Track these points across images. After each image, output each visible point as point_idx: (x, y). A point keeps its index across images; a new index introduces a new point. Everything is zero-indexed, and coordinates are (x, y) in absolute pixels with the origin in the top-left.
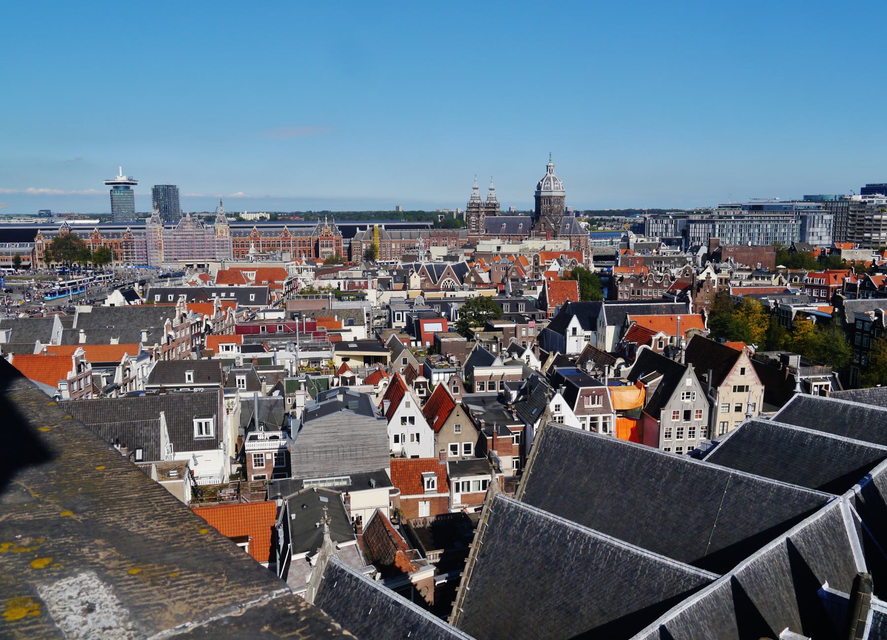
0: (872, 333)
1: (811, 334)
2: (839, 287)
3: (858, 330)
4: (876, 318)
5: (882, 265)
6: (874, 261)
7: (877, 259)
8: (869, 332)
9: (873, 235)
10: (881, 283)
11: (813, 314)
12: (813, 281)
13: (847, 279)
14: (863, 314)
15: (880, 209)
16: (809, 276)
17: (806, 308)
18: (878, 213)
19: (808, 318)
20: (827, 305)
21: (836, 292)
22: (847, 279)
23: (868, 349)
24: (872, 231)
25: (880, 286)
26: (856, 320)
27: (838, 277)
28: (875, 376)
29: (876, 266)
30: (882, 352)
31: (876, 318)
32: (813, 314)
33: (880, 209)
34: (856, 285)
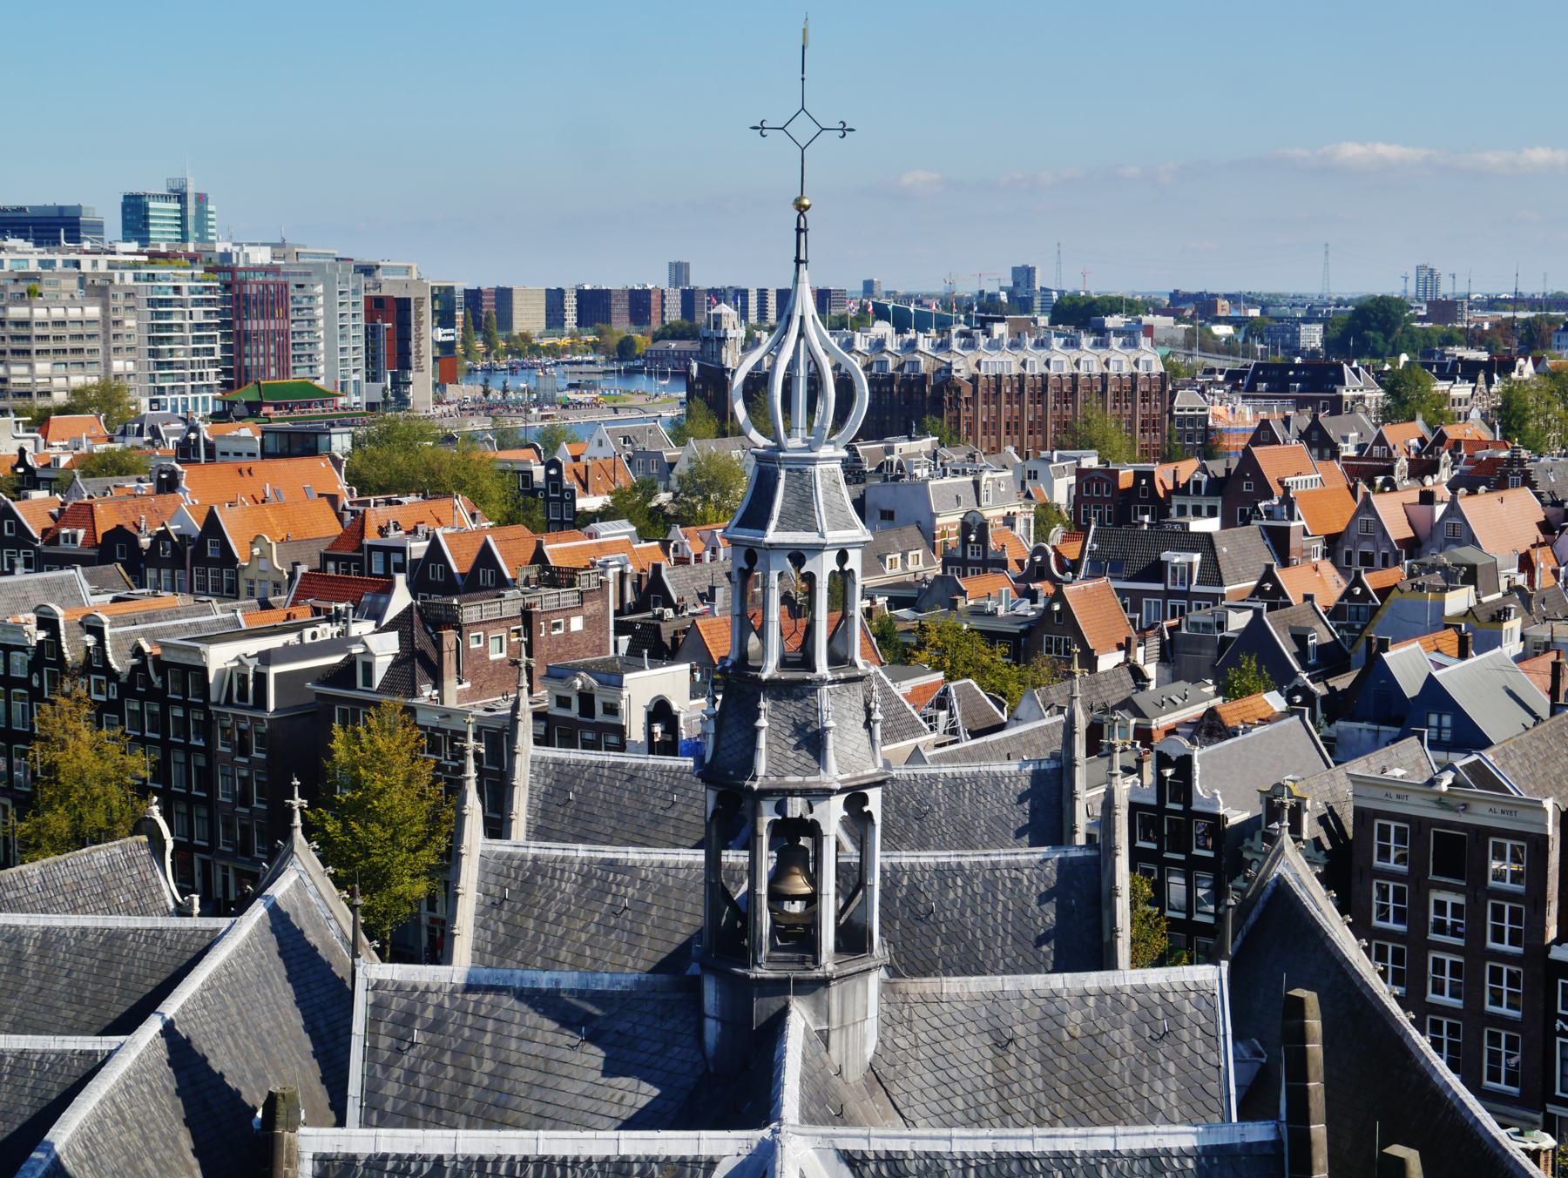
0: (35, 683)
4: (42, 635)
5: (48, 466)
6: (22, 452)
7: (29, 447)
8: (25, 683)
9: (14, 370)
10: (49, 523)
15: (23, 287)
18: (21, 299)
23: (29, 737)
24: (9, 357)
25: (45, 532)
28: (58, 821)
29: (30, 470)
30: (71, 741)
31: (42, 635)
33: (23, 287)
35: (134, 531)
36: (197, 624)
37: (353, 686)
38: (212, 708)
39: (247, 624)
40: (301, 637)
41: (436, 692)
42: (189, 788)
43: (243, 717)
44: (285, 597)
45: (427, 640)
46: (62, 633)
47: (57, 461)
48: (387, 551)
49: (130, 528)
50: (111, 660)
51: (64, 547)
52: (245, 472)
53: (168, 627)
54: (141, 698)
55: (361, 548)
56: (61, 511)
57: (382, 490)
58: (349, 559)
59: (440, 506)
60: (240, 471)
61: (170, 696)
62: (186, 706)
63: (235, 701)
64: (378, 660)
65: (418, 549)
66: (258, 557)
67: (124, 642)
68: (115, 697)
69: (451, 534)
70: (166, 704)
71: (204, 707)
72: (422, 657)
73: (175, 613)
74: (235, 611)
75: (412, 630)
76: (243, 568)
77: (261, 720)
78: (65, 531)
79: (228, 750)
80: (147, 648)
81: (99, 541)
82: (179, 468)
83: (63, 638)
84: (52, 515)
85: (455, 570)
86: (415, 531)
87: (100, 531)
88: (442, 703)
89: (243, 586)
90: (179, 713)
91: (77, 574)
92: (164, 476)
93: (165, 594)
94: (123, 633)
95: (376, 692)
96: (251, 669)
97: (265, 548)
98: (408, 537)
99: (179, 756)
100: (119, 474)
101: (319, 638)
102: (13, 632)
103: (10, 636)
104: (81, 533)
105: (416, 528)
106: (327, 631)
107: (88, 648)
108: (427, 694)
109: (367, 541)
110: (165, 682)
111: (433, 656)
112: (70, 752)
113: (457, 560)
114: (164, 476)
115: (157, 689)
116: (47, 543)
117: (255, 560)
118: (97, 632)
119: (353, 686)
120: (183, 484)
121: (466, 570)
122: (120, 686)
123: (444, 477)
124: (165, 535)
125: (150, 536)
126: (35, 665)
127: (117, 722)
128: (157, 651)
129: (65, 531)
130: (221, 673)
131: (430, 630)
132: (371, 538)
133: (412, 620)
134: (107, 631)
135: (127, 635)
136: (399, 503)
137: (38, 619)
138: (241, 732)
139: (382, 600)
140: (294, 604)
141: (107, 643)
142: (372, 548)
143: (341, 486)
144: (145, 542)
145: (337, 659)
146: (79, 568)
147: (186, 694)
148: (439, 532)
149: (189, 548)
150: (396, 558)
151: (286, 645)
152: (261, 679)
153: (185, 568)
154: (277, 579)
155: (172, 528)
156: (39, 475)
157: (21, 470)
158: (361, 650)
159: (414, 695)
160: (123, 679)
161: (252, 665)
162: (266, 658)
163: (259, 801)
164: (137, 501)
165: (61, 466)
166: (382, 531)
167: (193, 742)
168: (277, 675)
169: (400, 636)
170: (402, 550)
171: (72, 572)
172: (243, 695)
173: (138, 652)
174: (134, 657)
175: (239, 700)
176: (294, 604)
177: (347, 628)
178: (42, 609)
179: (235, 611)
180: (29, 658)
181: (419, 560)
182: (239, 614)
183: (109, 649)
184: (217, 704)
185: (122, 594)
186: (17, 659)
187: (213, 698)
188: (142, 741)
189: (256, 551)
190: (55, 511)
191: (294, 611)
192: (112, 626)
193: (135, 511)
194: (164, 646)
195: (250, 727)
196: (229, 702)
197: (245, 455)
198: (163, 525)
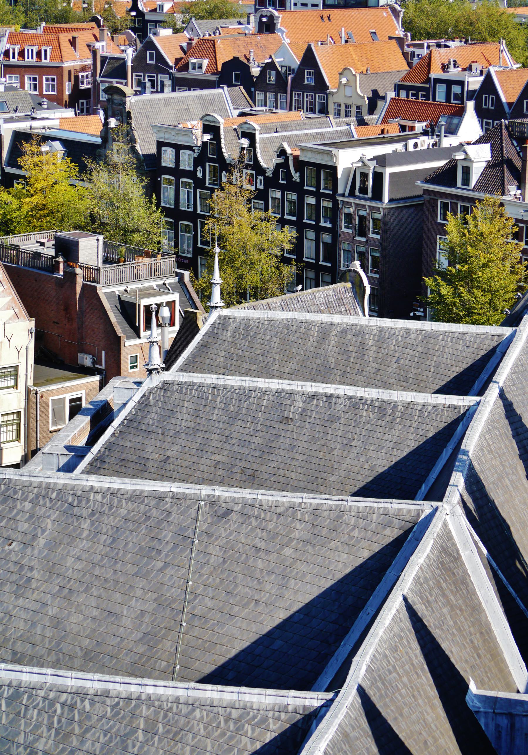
0: (200, 175)
1: (63, 187)
2: (84, 69)
3: (167, 171)
4: (207, 137)
5: (154, 10)
8: (192, 174)
10: (181, 55)
11: (54, 139)
12: (22, 54)
13: (98, 45)
14: (174, 128)
16: (11, 41)
17: (35, 124)
19: (45, 148)
20: (69, 113)
21: (77, 78)
22: (98, 45)
25: (178, 61)
26: (160, 145)
27: (78, 42)
30: (236, 219)
31: (207, 137)
32: (54, 139)
34: (123, 62)
35: (245, 61)
36: (322, 134)
37: (453, 184)
38: (338, 198)
39: (358, 135)
40: (406, 146)
41: (519, 192)
42: (317, 259)
43: (364, 206)
44: (377, 116)
45: (514, 152)
46: (222, 136)
47: (161, 7)
48: (449, 83)
49: (243, 59)
50: (260, 159)
51: (192, 74)
52: (326, 18)
53: (301, 135)
54: (283, 189)
55: (428, 80)
56: (189, 45)
57: (430, 36)
58: (418, 89)
59: (489, 49)
60: (322, 18)
61: (305, 188)
62: (318, 195)
63: (357, 193)
64: (475, 165)
65: (475, 82)
66: (345, 85)
67: (269, 145)
68: (262, 187)
69: (501, 72)
70: (302, 194)
71: (333, 197)
72: (509, 163)
73: (301, 126)
74: (349, 125)
75: (502, 142)
76: (333, 94)
77: (378, 209)
78: (193, 60)
79: (350, 231)
80: (289, 151)
81: (220, 69)
82: (276, 13)
83: (222, 141)
84: (182, 48)
85: (504, 100)
86: (470, 68)
87: (220, 62)
88: (524, 200)
89: (332, 107)
90: (312, 200)
91: (224, 92)
92: (264, 20)
93: (282, 111)
94: (268, 138)
95: (473, 191)
96: (372, 169)
97: (351, 78)
98: (466, 73)
99: (310, 234)
100: (221, 17)
101: (419, 148)
102: (183, 135)
103: (181, 138)
104: (205, 63)
105: (471, 66)
106: (425, 142)
107: (242, 149)
108: (512, 193)
109: (433, 75)
110: (302, 177)
111: (518, 164)
112: (236, 226)
113: (505, 92)
114: (264, 20)
115: (296, 182)
116: (180, 70)
117: (342, 87)
118: (251, 137)
119: (453, 184)
120: (279, 26)
121: (514, 99)
122: (266, 179)
123: (481, 27)
124: (271, 66)
125: (258, 66)
126: (199, 162)
127: (262, 207)
128: (297, 153)
129: (193, 60)
130: (347, 171)
131: (516, 144)
132: (436, 73)
133: (502, 135)
134: (258, 137)
135: (271, 140)
136: (446, 46)
137: (204, 125)
138: (362, 218)
139: (455, 121)
140: (385, 121)
141: (258, 145)
142: (437, 81)
143: (400, 32)
144: (255, 71)
145: (440, 164)
146: (226, 87)
147: (318, 187)
148: (493, 70)
149: (290, 78)
150: (456, 89)
151: (395, 152)
152: (378, 177)
153: (286, 92)
154: (359, 103)
155: (277, 60)
156: (147, 18)
157: (133, 13)
158: (462, 157)
159: (503, 193)
160: (269, 174)
161: (372, 165)
162: (381, 160)
163: (371, 272)
164: (247, 39)
165: (165, 10)
166: (445, 68)
167: (322, 224)
168: (391, 175)
169: (492, 147)
170: (461, 83)
171: (220, 90)
172: (364, 190)
173: (282, 153)
174: (278, 156)
175: (360, 193)
176: (385, 121)
177: (440, 140)
178: (206, 118)
179: (349, 125)
180: (196, 155)
181: (475, 91)
182: (352, 127)
183: (258, 150)
184: (343, 195)
185: (247, 110)
186: (185, 154)
187: (340, 191)
188: (282, 222)
189: (344, 81)
190: (184, 45)
191: (386, 127)
192: (261, 133)
193: (246, 45)
194: (302, 149)
195: (368, 214)
196: (352, 194)
197: (309, 5)
198: (271, 57)
